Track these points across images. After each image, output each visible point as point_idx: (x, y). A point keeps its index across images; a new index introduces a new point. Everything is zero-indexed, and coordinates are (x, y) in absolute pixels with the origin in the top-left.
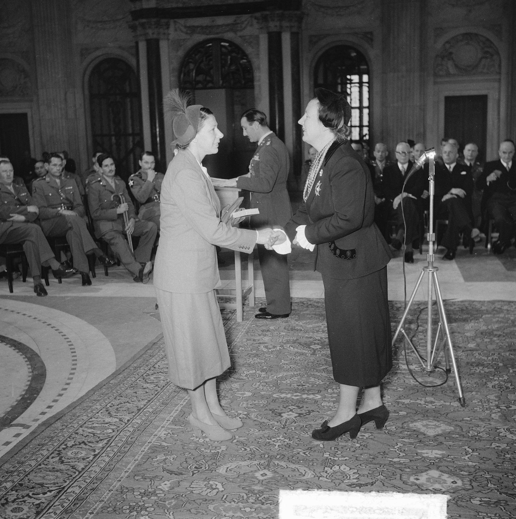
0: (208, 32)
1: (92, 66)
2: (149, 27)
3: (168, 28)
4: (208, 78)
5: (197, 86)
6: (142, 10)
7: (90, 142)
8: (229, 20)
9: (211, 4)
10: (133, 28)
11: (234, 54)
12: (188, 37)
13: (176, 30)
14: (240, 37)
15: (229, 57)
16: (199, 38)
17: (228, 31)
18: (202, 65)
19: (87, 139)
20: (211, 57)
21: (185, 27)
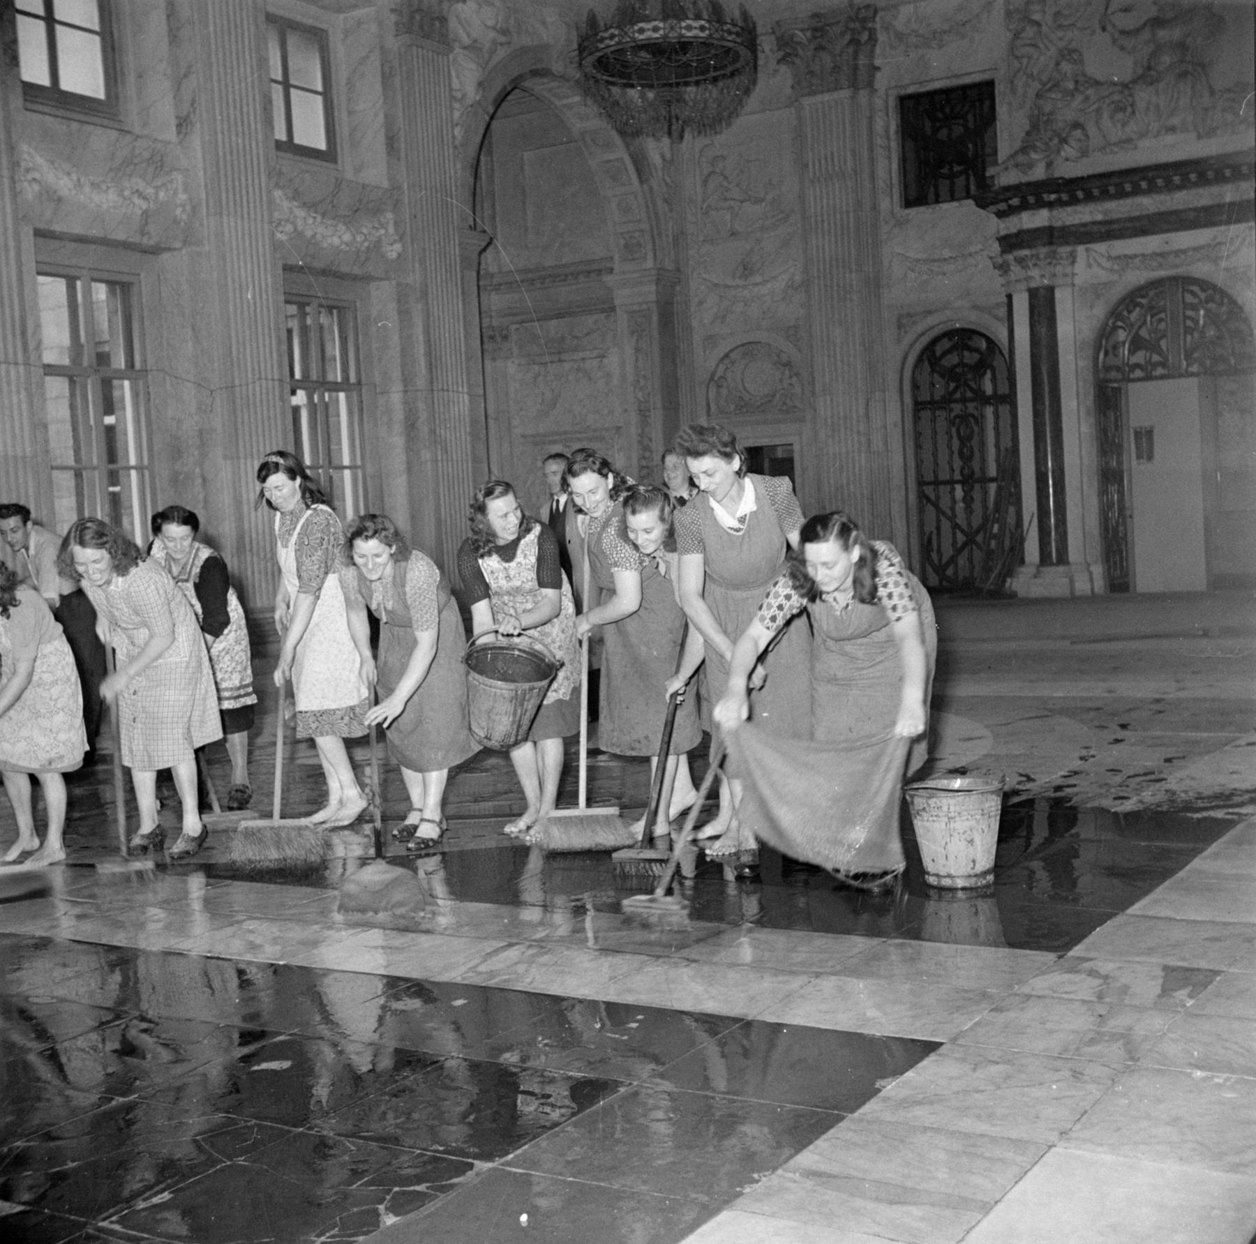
0: (1155, 264)
1: (919, 347)
2: (1035, 265)
3: (1073, 263)
4: (1156, 358)
5: (1132, 376)
6: (1020, 233)
7: (913, 497)
8: (1202, 236)
9: (1163, 209)
10: (1003, 268)
11: (1211, 305)
12: (1115, 277)
13: (1089, 266)
14: (1227, 270)
15: (1202, 312)
16: (1136, 277)
17: (1199, 260)
18: (1143, 333)
19: (907, 489)
20: (1163, 315)
21: (1109, 258)
